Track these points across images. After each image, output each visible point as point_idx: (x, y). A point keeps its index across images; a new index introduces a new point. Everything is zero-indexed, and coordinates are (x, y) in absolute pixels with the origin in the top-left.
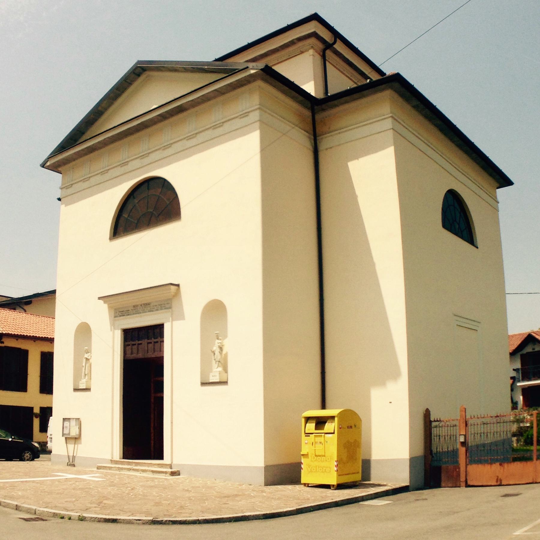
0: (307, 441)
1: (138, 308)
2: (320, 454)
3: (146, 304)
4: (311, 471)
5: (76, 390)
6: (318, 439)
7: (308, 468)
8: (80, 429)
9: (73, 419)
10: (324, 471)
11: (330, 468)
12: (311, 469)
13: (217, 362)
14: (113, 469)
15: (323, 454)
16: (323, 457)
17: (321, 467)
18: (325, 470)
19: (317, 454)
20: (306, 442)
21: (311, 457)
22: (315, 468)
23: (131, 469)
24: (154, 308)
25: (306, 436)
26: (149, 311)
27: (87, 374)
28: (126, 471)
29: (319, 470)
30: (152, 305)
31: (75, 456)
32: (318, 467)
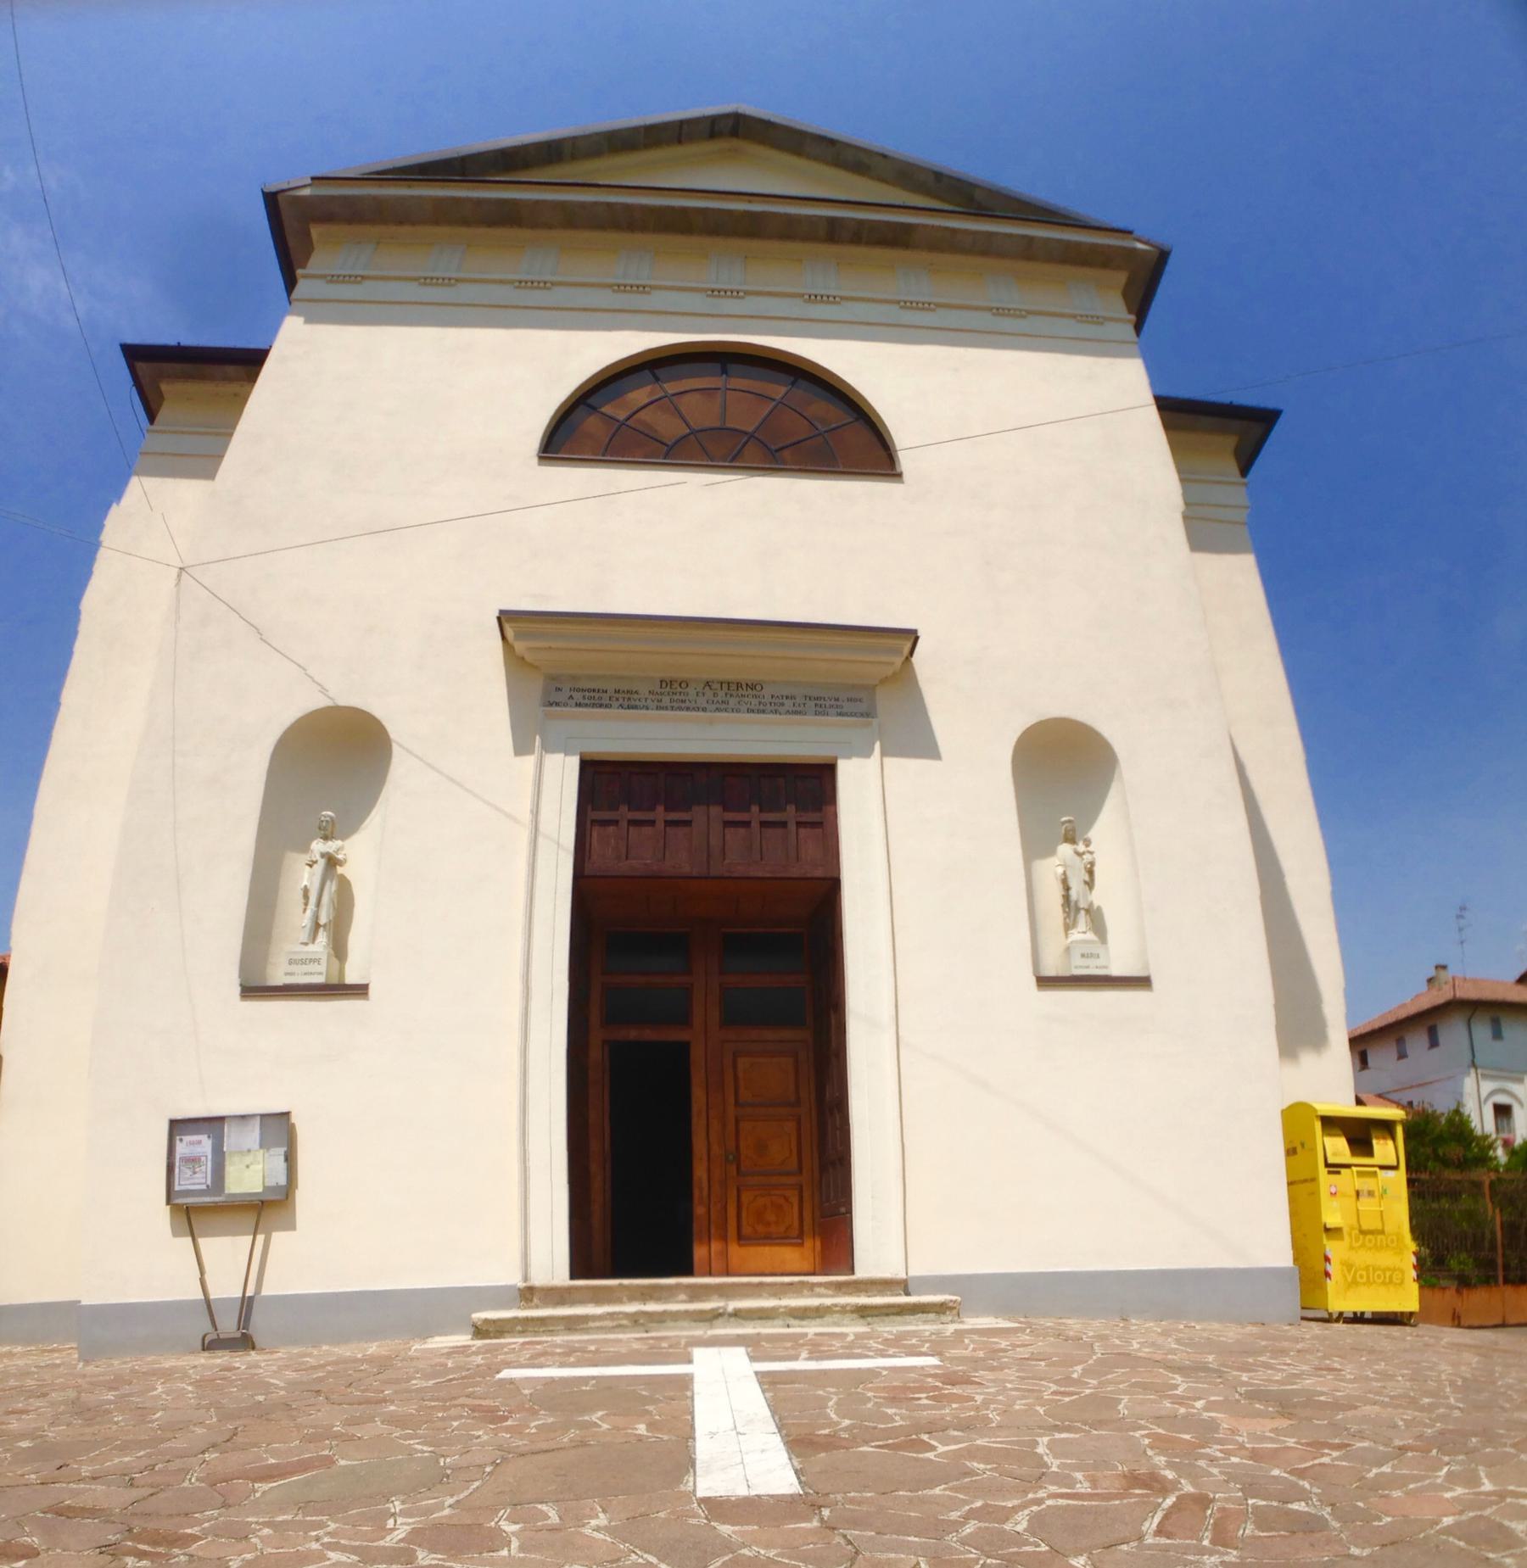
0: (1335, 1186)
1: (691, 691)
2: (1372, 1227)
3: (739, 685)
4: (1354, 1283)
5: (253, 990)
6: (1365, 1184)
7: (1347, 1275)
8: (290, 1159)
9: (243, 1117)
10: (1387, 1280)
11: (1402, 1272)
12: (1354, 1277)
13: (1083, 912)
14: (591, 1324)
15: (1380, 1227)
16: (1379, 1237)
17: (1379, 1269)
18: (1391, 1277)
19: (1365, 1227)
20: (1333, 1190)
21: (1350, 1235)
22: (1364, 1273)
23: (721, 1315)
24: (783, 704)
25: (1329, 1172)
26: (750, 711)
27: (325, 926)
28: (685, 1324)
29: (1376, 1278)
30: (767, 692)
31: (251, 1298)
32: (1371, 1269)
